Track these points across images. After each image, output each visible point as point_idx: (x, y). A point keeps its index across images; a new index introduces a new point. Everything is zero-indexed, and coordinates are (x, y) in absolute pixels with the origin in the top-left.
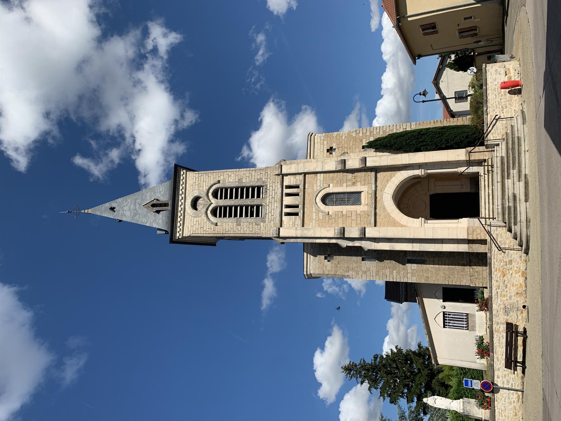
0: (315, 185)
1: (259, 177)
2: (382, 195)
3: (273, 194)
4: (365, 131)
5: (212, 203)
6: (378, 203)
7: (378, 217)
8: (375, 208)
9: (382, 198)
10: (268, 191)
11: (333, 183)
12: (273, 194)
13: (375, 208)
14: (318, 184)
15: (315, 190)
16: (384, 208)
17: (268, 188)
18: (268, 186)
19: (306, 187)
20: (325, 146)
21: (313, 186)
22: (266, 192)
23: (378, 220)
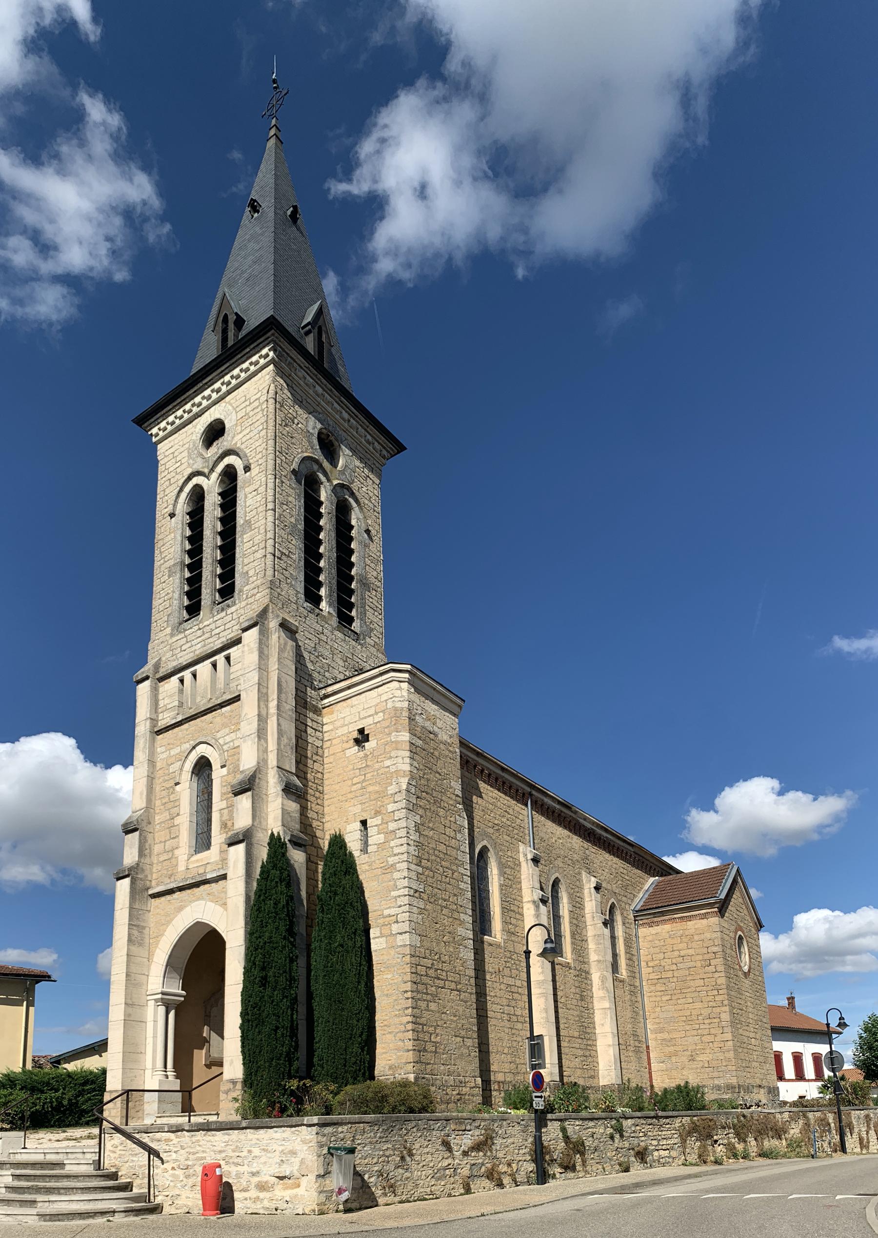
0: (227, 730)
1: (251, 573)
2: (203, 899)
3: (217, 631)
4: (398, 815)
5: (208, 478)
6: (188, 891)
7: (168, 897)
8: (181, 889)
9: (198, 899)
10: (223, 614)
11: (229, 774)
12: (217, 631)
13: (181, 889)
14: (228, 739)
15: (219, 735)
16: (180, 909)
17: (230, 611)
18: (233, 609)
19: (224, 709)
20: (370, 721)
21: (224, 726)
22: (223, 610)
23: (163, 899)
